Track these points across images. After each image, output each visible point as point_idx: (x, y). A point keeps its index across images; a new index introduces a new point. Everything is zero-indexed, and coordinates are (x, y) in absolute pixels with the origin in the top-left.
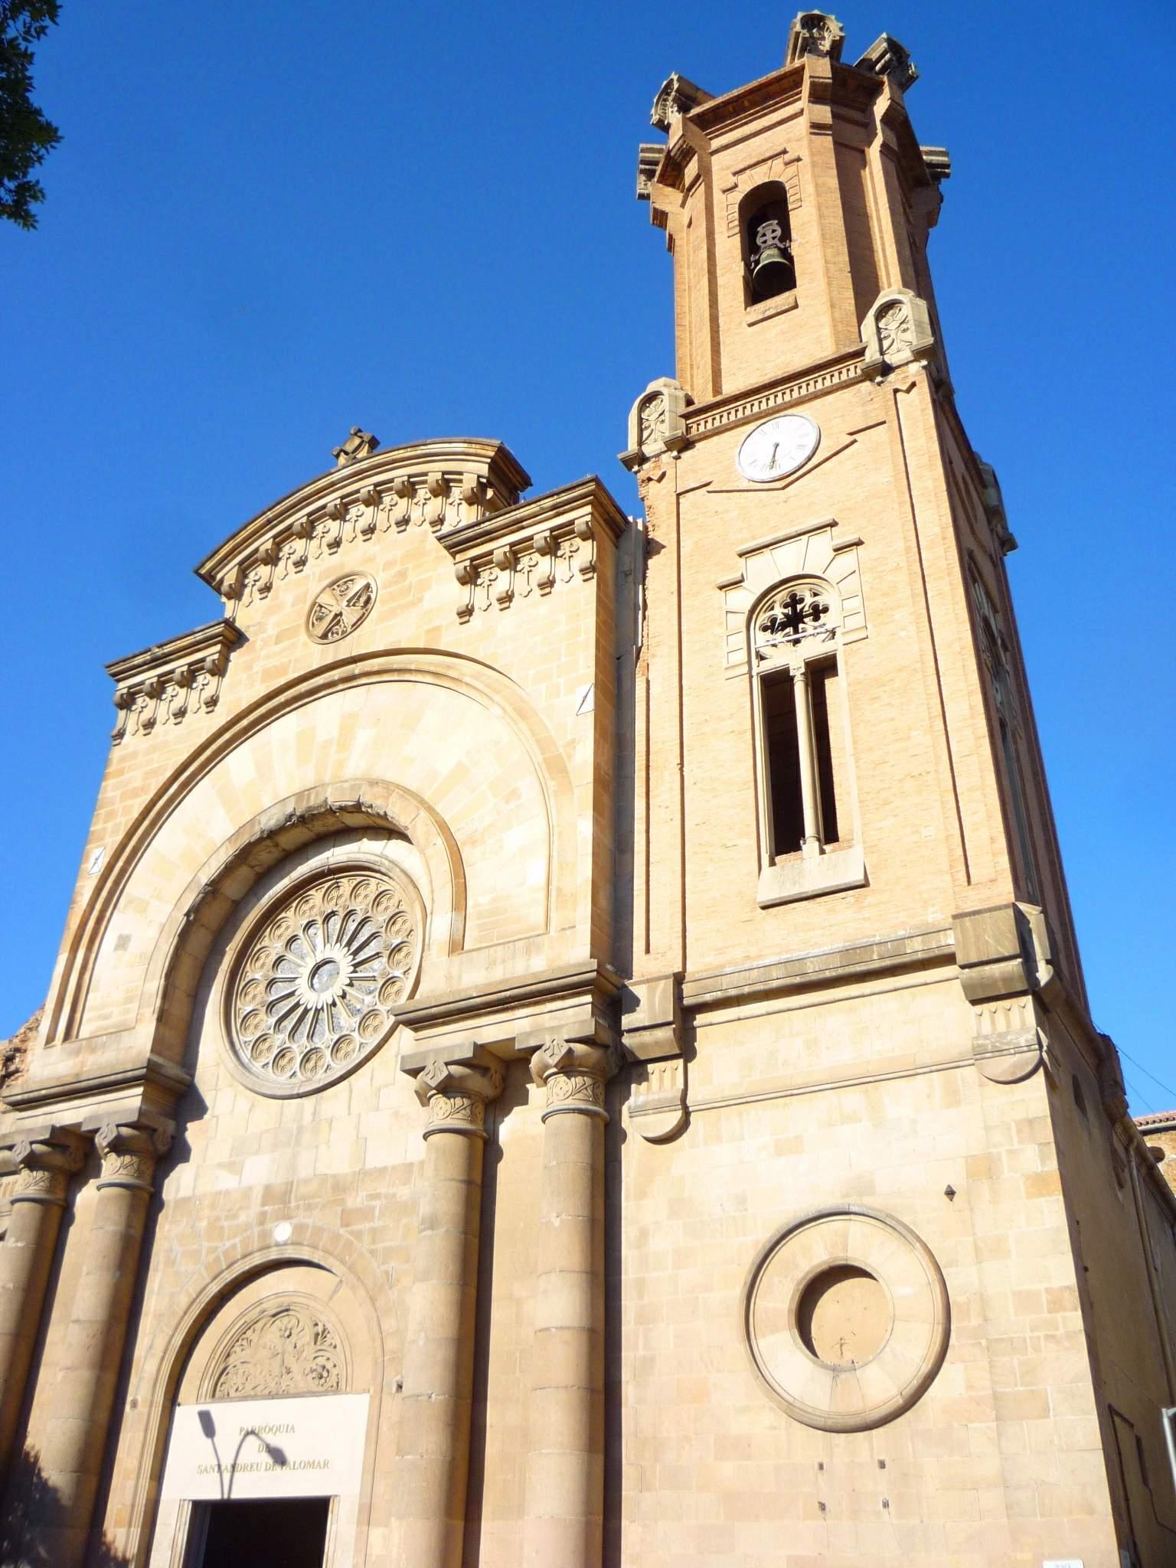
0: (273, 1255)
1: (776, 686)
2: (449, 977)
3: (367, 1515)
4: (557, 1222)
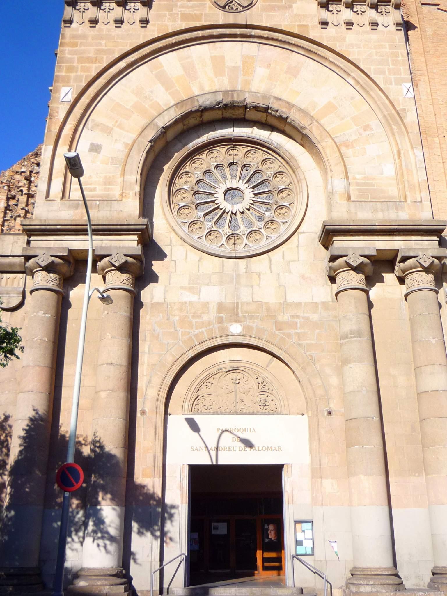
0: (231, 340)
2: (349, 212)
3: (317, 473)
4: (434, 342)
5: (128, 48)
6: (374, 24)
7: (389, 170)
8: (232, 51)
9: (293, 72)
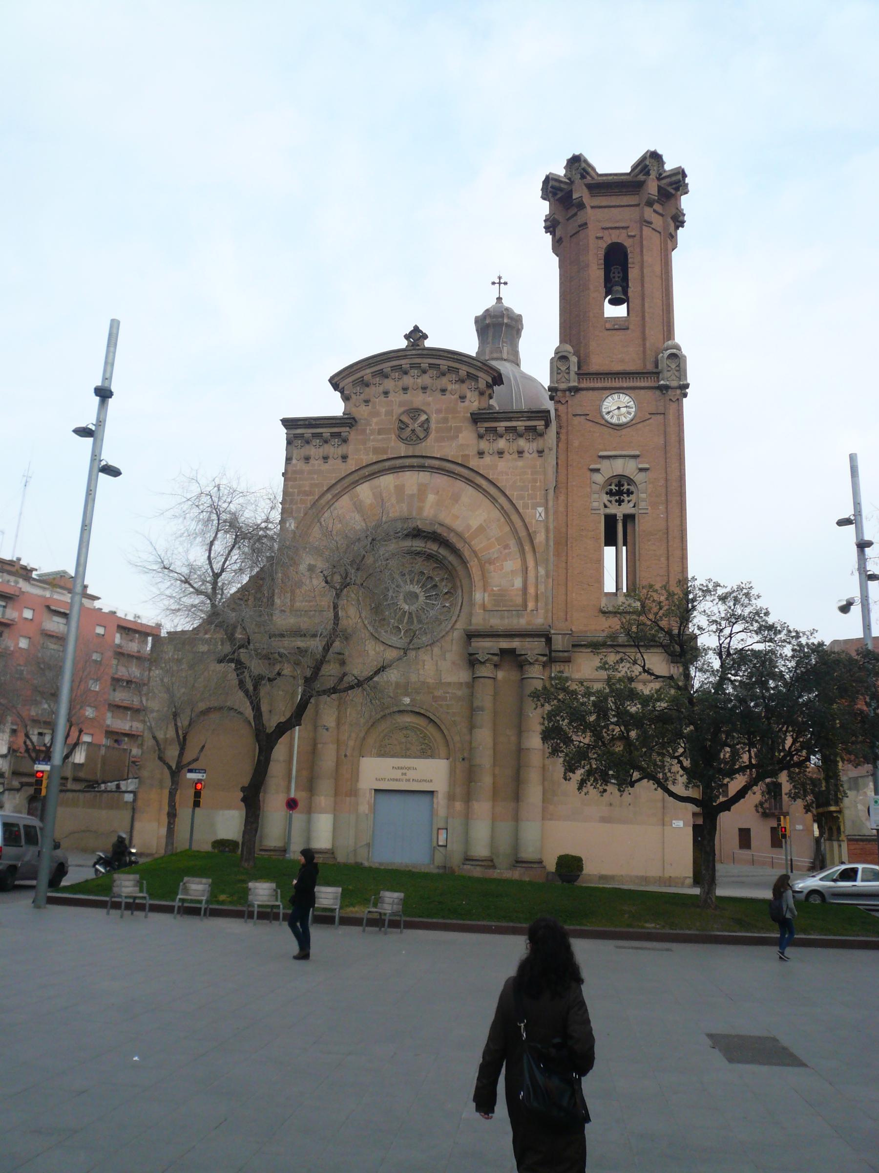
1: (611, 521)
2: (484, 619)
5: (333, 482)
6: (520, 453)
7: (518, 583)
8: (411, 480)
9: (456, 498)
